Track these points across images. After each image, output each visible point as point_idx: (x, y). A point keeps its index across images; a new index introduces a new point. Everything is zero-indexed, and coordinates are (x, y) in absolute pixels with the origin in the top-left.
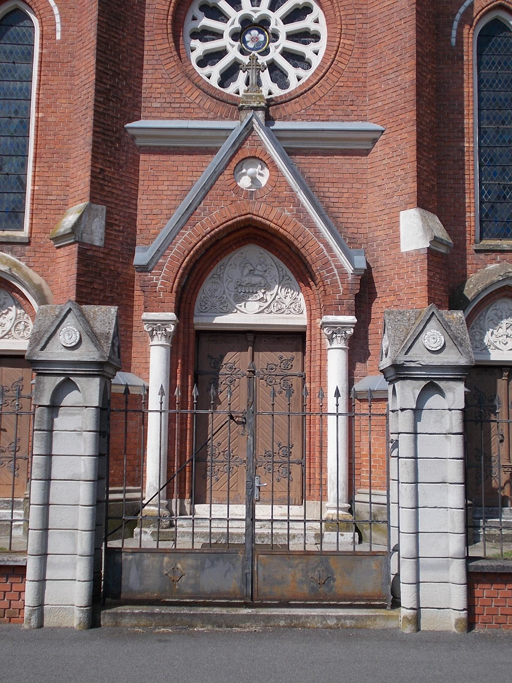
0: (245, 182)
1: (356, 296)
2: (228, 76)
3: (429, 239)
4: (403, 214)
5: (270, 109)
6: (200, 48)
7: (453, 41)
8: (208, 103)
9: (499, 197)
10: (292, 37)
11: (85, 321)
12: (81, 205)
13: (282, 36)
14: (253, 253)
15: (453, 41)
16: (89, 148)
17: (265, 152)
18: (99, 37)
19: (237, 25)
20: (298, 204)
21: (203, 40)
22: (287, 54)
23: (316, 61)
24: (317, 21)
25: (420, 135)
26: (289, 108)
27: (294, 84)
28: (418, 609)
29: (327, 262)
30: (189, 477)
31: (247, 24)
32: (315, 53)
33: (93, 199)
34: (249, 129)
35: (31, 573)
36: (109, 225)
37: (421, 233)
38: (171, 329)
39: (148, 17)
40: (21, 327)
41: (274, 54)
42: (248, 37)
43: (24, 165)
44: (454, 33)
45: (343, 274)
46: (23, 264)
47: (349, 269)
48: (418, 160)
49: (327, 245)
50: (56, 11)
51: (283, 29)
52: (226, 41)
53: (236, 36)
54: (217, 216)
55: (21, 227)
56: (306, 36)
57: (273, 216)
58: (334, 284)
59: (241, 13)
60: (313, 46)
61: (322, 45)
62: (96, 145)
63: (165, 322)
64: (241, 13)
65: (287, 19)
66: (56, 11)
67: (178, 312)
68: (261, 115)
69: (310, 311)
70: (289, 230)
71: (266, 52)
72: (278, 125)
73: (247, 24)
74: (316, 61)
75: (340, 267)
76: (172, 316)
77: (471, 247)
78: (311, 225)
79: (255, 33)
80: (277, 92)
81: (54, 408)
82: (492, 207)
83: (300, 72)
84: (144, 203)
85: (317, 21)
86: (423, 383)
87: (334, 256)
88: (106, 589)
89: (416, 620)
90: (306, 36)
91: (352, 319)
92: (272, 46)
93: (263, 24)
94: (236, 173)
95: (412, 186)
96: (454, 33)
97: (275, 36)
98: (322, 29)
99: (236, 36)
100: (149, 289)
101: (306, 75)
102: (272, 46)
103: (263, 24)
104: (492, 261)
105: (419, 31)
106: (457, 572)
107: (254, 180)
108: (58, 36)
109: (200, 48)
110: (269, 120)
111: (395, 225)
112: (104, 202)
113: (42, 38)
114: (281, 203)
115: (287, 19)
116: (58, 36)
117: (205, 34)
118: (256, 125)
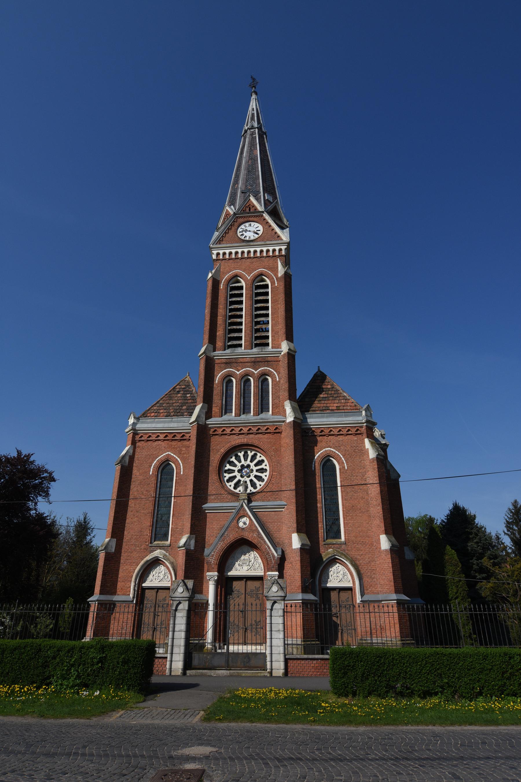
0: (241, 524)
1: (279, 564)
2: (236, 486)
3: (300, 544)
4: (293, 535)
5: (250, 498)
6: (227, 476)
7: (313, 468)
8: (230, 497)
9: (333, 523)
10: (257, 471)
11: (185, 585)
12: (187, 535)
13: (255, 471)
14: (245, 548)
15: (313, 468)
16: (190, 516)
17: (247, 513)
18: (194, 479)
19: (240, 468)
20: (258, 532)
21: (229, 473)
22: (256, 476)
23: (266, 479)
24: (266, 465)
25: (297, 507)
26: (256, 497)
27: (259, 487)
28: (272, 669)
29: (268, 553)
30: (222, 635)
31: (243, 466)
32: (265, 476)
33: (191, 534)
34: (242, 506)
35: (168, 659)
36: (196, 542)
38: (216, 578)
39: (211, 468)
40: (166, 577)
42: (243, 471)
43: (169, 517)
44: (313, 466)
45: (274, 556)
46: (167, 554)
47: (276, 554)
48: (297, 516)
49: (268, 546)
50: (181, 465)
51: (255, 469)
52: (236, 473)
53: (239, 471)
54: (231, 537)
55: (167, 540)
56: (262, 471)
58: (271, 561)
59: (241, 464)
60: (265, 474)
61: (267, 473)
62: (192, 515)
63: (214, 576)
64: (241, 464)
65: (256, 465)
66: (181, 465)
67: (218, 572)
68: (246, 501)
69: (264, 569)
70: (255, 541)
71: (249, 476)
72: (253, 504)
73: (243, 466)
74: (266, 479)
76: (216, 573)
77: (321, 543)
78: (263, 540)
79: (246, 469)
80: (254, 491)
81: (176, 610)
82: (331, 527)
83: (261, 483)
84: (208, 532)
85: (266, 465)
86: (273, 601)
87: (271, 550)
88: (188, 665)
89: (271, 673)
90: (262, 471)
91: (277, 573)
92: (251, 474)
93: (248, 466)
94: (238, 523)
96: (313, 466)
97: (252, 471)
98: (268, 468)
99: (239, 471)
100: (209, 563)
101: (263, 484)
102: (251, 474)
103: (248, 466)
104: (330, 548)
105: (296, 471)
106: (282, 658)
107: (245, 523)
108: (182, 473)
109: (227, 476)
110: (250, 501)
111: (291, 538)
112: (194, 534)
113: (176, 474)
114: (253, 531)
115: (256, 465)
116: (182, 473)
117: (230, 471)
118: (244, 505)
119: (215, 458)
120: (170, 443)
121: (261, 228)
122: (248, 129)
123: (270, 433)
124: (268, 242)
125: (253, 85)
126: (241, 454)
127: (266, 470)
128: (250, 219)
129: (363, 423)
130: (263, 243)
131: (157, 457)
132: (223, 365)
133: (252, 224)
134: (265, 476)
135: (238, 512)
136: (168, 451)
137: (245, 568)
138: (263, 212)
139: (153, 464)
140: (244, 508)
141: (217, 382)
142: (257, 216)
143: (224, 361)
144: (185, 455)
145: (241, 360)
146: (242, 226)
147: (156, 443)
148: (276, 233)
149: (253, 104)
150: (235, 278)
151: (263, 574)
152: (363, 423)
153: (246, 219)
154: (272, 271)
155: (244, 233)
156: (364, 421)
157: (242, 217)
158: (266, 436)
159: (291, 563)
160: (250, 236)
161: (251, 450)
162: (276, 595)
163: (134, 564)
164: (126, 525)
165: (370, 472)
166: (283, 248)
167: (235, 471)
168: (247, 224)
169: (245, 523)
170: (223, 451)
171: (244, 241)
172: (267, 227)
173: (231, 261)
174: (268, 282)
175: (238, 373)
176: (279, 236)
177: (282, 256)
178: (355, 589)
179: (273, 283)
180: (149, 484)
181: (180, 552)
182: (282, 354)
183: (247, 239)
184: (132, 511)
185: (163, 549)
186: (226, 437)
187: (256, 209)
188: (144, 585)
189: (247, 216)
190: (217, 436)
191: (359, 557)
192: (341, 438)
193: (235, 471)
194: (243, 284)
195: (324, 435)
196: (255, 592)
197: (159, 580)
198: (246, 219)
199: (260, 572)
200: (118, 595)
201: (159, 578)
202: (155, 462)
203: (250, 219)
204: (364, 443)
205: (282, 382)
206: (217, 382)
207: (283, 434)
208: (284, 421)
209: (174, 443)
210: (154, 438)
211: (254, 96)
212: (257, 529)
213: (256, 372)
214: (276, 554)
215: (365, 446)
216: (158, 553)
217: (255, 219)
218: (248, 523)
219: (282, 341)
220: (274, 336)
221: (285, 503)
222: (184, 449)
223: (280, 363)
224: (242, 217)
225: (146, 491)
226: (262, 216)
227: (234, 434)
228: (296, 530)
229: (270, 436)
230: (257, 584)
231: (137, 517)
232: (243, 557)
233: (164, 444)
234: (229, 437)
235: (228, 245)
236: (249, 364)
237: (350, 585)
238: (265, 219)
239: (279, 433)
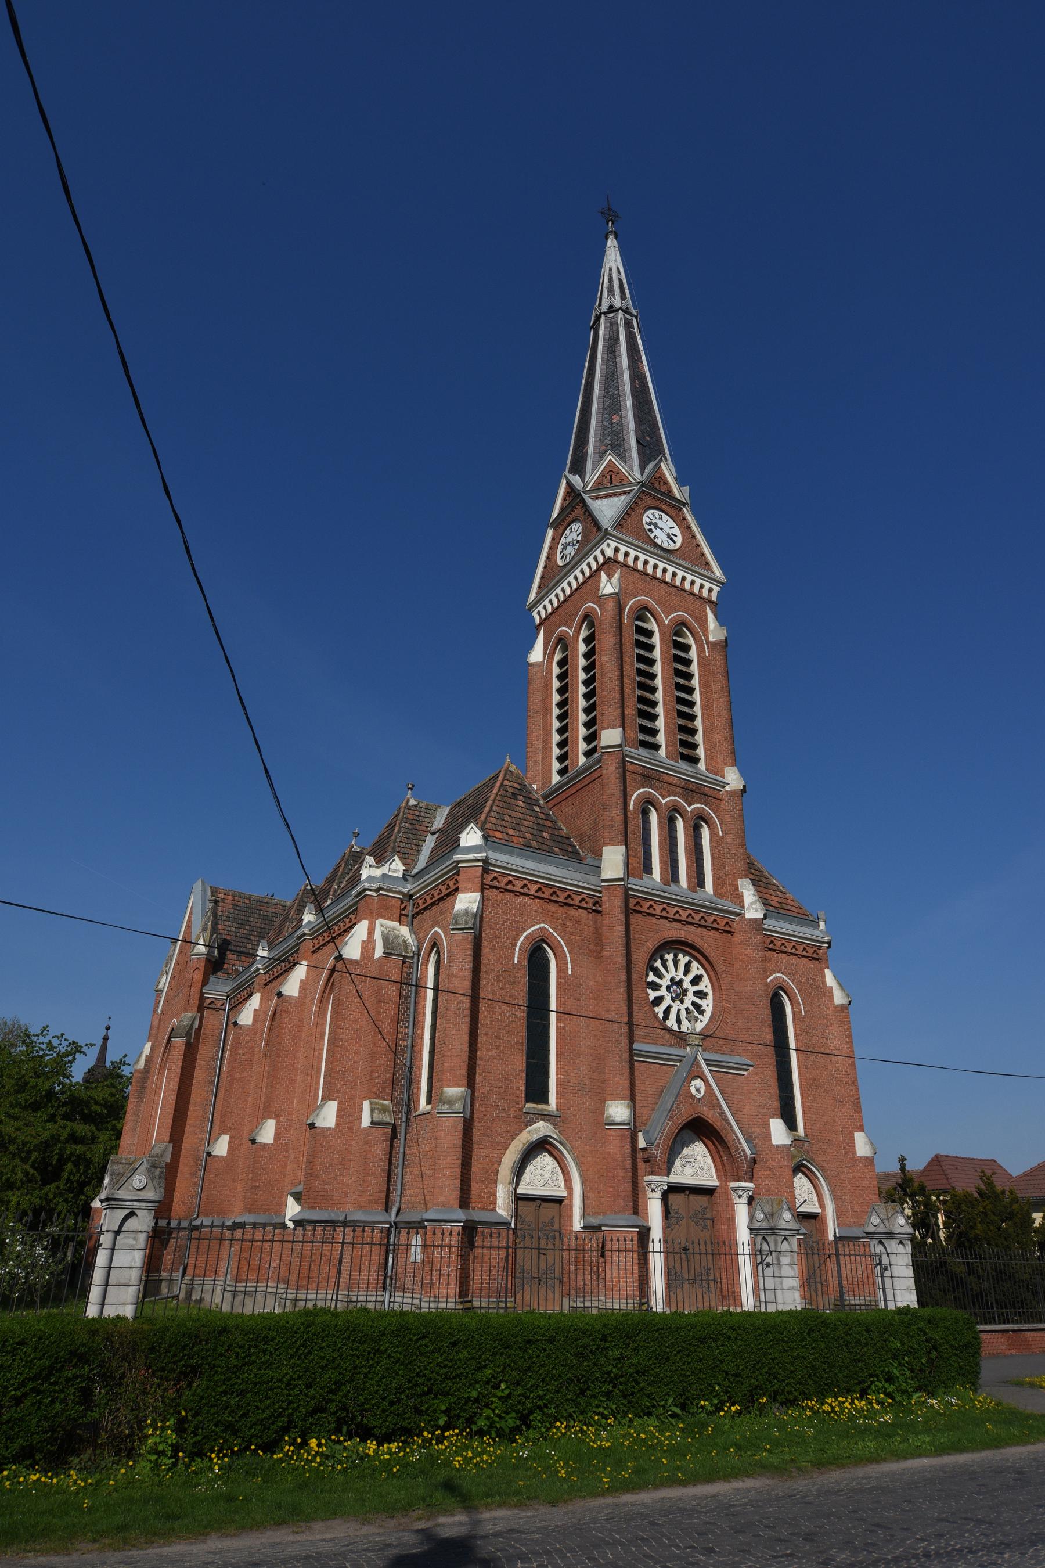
4: (771, 1120)
13: (690, 994)
17: (703, 1072)
20: (721, 1109)
37: (785, 1135)
41: (687, 1003)
45: (745, 1154)
47: (749, 1152)
53: (668, 988)
54: (685, 1114)
57: (710, 1115)
70: (718, 1125)
75: (744, 1151)
93: (681, 982)
95: (777, 1105)
98: (709, 990)
103: (681, 982)
107: (698, 1090)
117: (655, 987)
119: (640, 957)
120: (546, 905)
121: (676, 531)
122: (621, 308)
123: (717, 929)
124: (696, 569)
125: (609, 215)
126: (670, 957)
127: (706, 994)
128: (664, 507)
129: (823, 943)
130: (689, 565)
131: (524, 930)
132: (639, 778)
133: (665, 517)
134: (708, 1005)
135: (690, 1071)
136: (543, 922)
137: (689, 1171)
138: (684, 504)
139: (519, 944)
140: (698, 1062)
141: (631, 808)
142: (673, 506)
143: (640, 770)
144: (572, 937)
145: (666, 778)
146: (649, 513)
147: (521, 899)
148: (703, 555)
149: (613, 259)
150: (642, 612)
151: (717, 1184)
152: (823, 943)
153: (656, 503)
154: (700, 626)
155: (652, 527)
156: (826, 939)
157: (651, 495)
158: (712, 933)
159: (770, 1169)
160: (661, 537)
161: (686, 953)
162: (903, 1230)
163: (499, 1147)
164: (478, 1062)
165: (835, 1027)
166: (716, 589)
167: (661, 986)
168: (657, 513)
169: (698, 1090)
170: (651, 945)
171: (656, 545)
172: (689, 536)
173: (637, 574)
174: (691, 641)
175: (663, 802)
176: (707, 564)
177: (712, 602)
178: (570, 1207)
179: (700, 650)
180: (514, 983)
181: (612, 1133)
182: (727, 788)
183: (659, 542)
184: (486, 1034)
185: (548, 1121)
186: (654, 920)
187: (670, 491)
188: (519, 1191)
189: (659, 499)
190: (639, 915)
191: (825, 1165)
192: (794, 960)
193: (661, 986)
194: (653, 626)
195: (774, 950)
196: (700, 1216)
197: (542, 1182)
198: (656, 503)
199: (711, 1179)
200: (474, 1209)
201: (543, 1177)
202: (522, 939)
203: (664, 507)
204: (824, 976)
205: (729, 839)
206: (631, 808)
207: (737, 938)
208: (739, 914)
209: (552, 908)
210: (518, 889)
211: (612, 242)
212: (719, 1103)
213: (689, 809)
214: (749, 1152)
215: (824, 982)
216: (541, 1129)
217: (669, 510)
218: (703, 1091)
219: (726, 765)
220: (710, 750)
221: (750, 1062)
222: (570, 924)
223: (723, 804)
224: (651, 495)
225: (510, 996)
226: (681, 510)
227: (666, 918)
228: (779, 1112)
229: (717, 934)
230: (703, 1200)
231: (498, 1048)
232: (686, 1151)
233: (535, 904)
234: (658, 922)
235: (636, 542)
236: (678, 790)
237: (816, 1209)
238: (684, 519)
239: (730, 932)
